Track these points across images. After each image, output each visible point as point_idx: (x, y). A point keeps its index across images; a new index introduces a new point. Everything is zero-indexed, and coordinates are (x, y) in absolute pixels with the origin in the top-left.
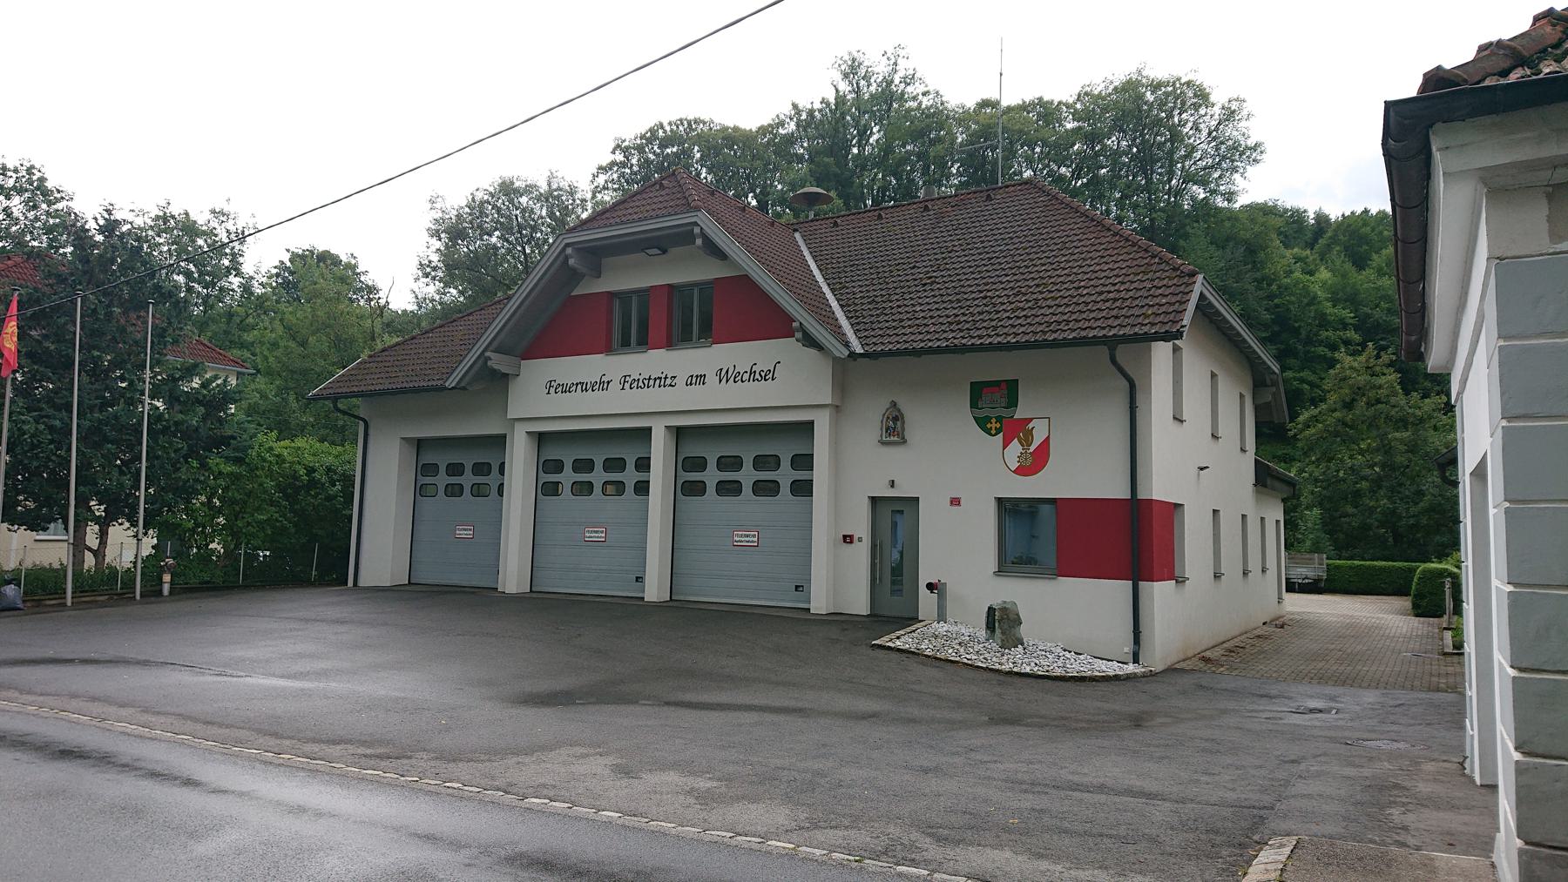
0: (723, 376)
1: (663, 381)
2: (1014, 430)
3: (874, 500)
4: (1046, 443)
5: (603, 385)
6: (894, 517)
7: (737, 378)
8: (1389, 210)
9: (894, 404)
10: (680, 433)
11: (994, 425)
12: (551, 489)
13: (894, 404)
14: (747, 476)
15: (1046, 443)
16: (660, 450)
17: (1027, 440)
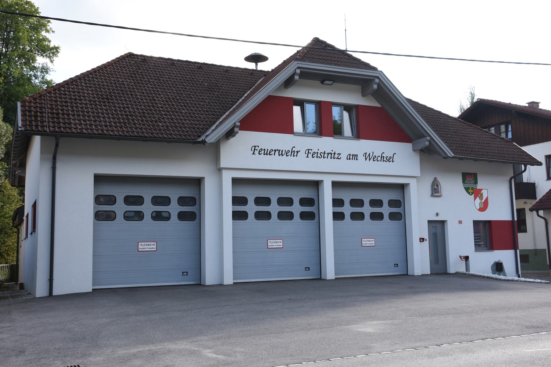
0: (368, 157)
1: (333, 155)
2: (477, 193)
3: (429, 222)
4: (487, 199)
5: (294, 153)
6: (437, 229)
7: (375, 159)
8: (62, 69)
9: (435, 179)
10: (336, 185)
11: (471, 191)
12: (238, 216)
13: (435, 179)
14: (274, 208)
15: (487, 199)
16: (327, 194)
17: (481, 198)
